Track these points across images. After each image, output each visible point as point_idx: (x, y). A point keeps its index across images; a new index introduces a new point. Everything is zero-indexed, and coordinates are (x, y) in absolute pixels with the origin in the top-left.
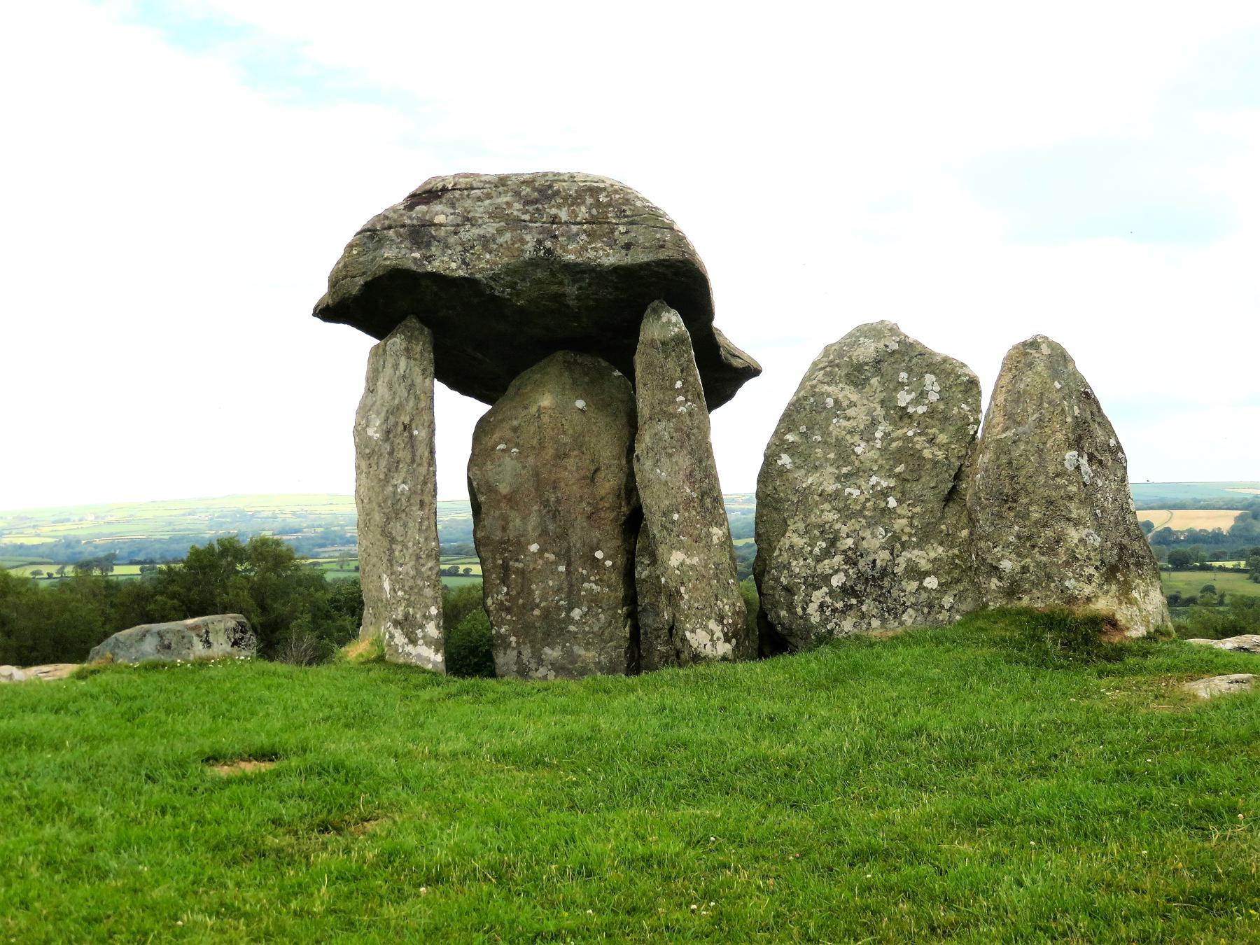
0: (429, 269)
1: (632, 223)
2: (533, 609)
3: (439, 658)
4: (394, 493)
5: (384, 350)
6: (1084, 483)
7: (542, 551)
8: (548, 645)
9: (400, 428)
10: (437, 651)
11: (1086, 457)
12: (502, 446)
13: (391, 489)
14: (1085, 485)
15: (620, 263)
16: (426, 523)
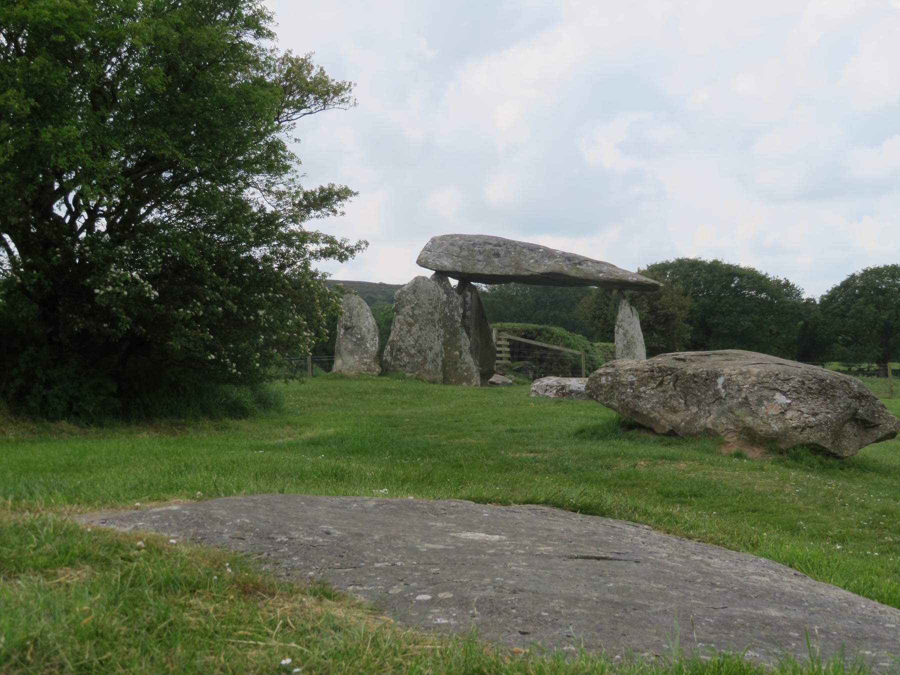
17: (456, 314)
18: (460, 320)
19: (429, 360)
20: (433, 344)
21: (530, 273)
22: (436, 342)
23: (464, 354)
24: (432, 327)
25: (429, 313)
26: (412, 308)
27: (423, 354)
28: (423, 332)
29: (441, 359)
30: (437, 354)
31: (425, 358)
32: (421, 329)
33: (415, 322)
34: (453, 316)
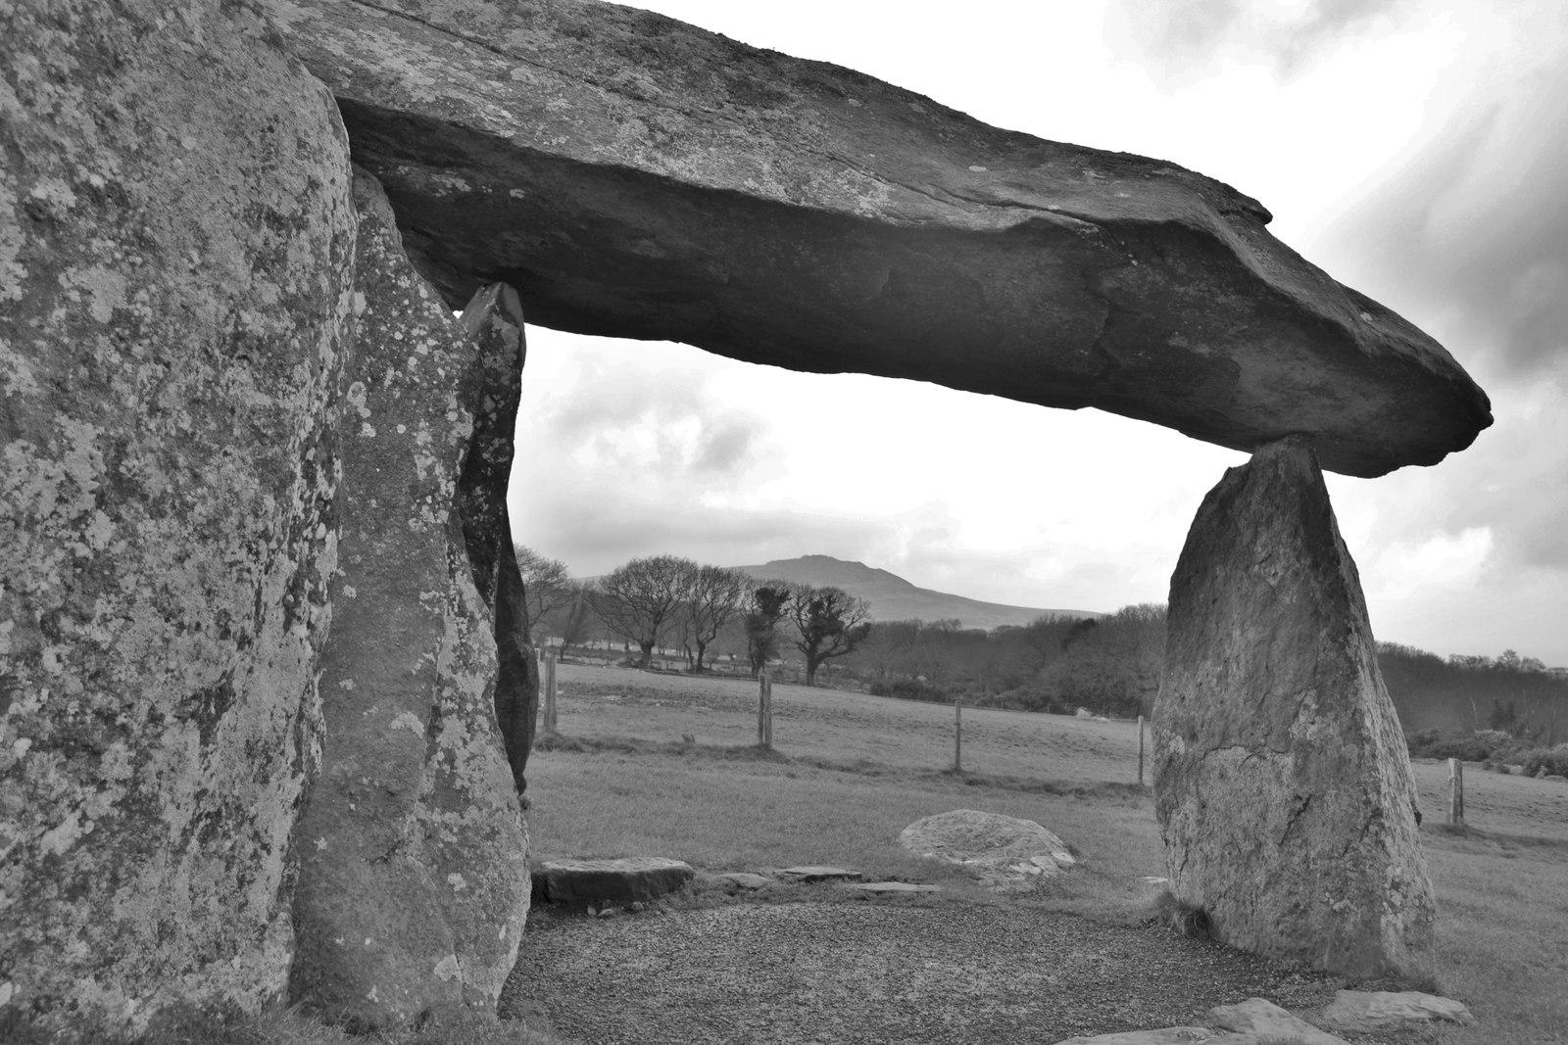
17: (423, 437)
18: (448, 487)
19: (176, 818)
20: (237, 659)
22: (268, 642)
23: (453, 727)
24: (248, 485)
25: (237, 343)
26: (36, 216)
27: (117, 759)
28: (147, 527)
29: (294, 788)
30: (258, 753)
31: (139, 807)
32: (119, 489)
33: (60, 397)
34: (406, 452)
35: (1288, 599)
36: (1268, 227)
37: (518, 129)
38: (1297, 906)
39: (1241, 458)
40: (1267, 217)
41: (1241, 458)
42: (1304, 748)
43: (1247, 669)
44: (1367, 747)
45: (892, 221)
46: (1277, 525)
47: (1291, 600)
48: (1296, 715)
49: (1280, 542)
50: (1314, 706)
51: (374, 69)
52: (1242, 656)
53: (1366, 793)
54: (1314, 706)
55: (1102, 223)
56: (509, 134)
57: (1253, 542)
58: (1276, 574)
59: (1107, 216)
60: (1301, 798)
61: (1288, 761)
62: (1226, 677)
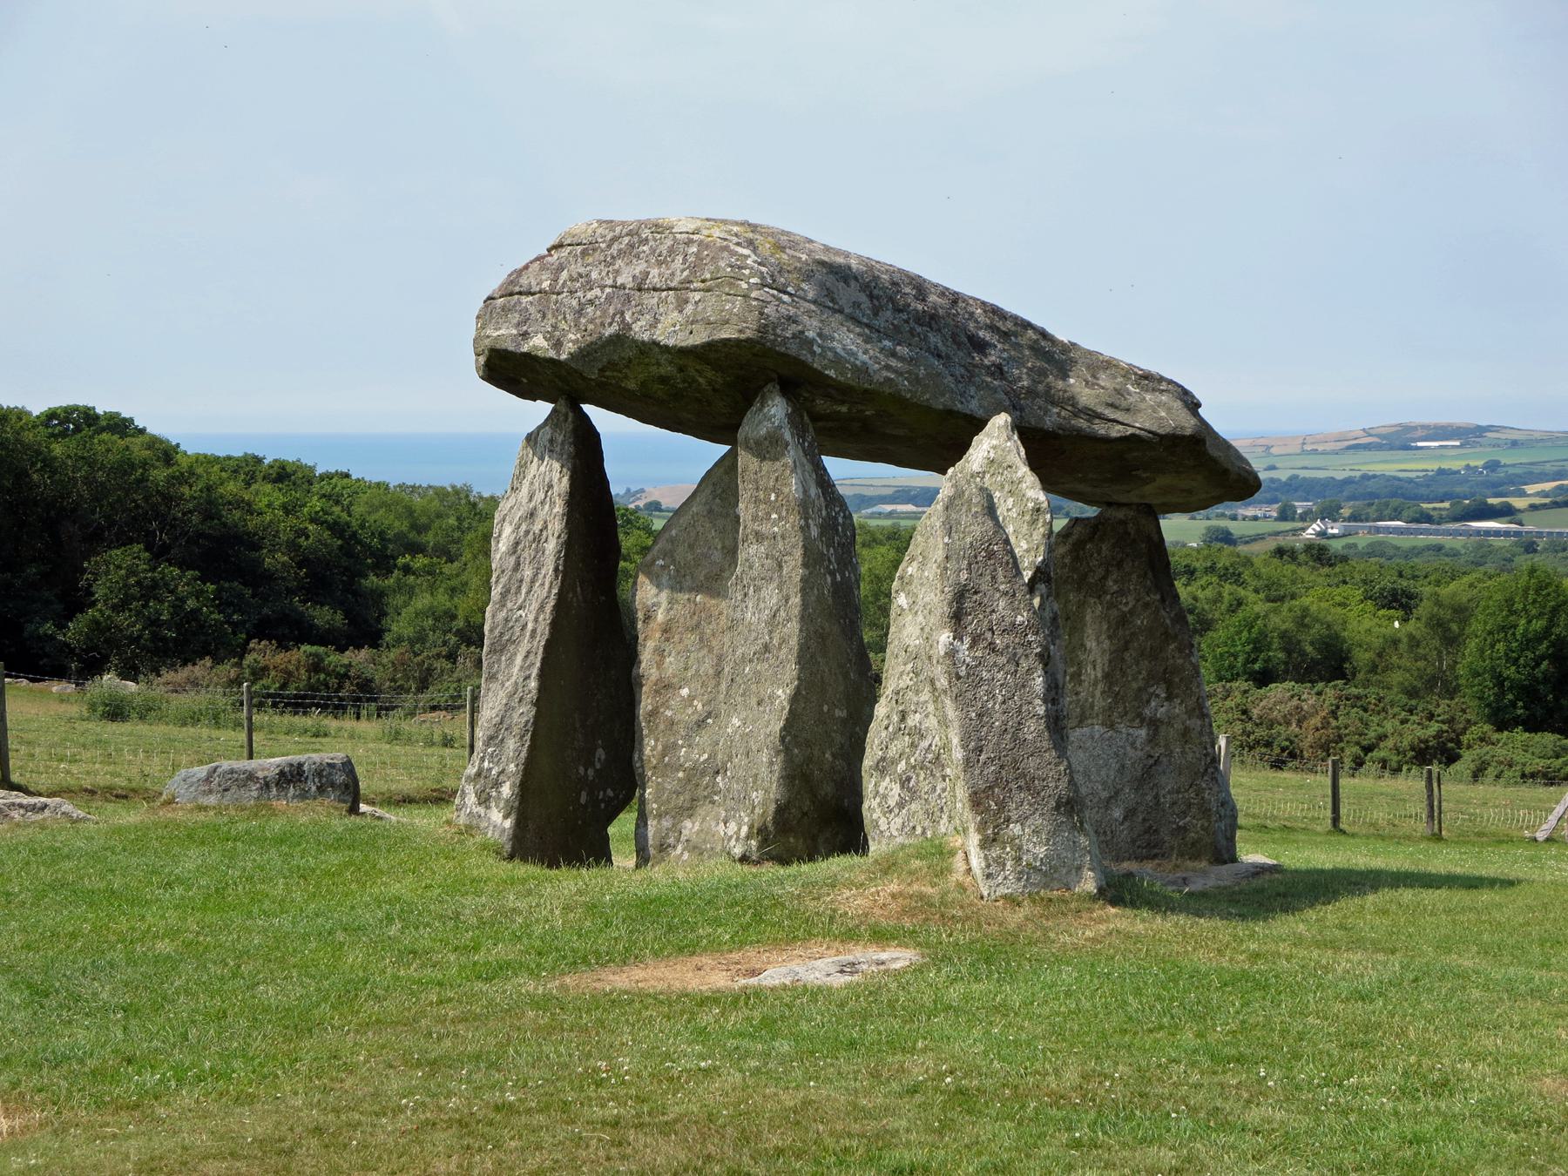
0: (525, 349)
1: (708, 290)
2: (678, 771)
3: (508, 824)
4: (507, 620)
5: (536, 439)
6: (957, 674)
7: (691, 698)
8: (690, 816)
9: (530, 537)
10: (506, 817)
11: (967, 640)
12: (661, 562)
13: (503, 614)
14: (959, 677)
15: (684, 344)
16: (532, 657)
21: (1116, 431)
35: (1139, 622)
36: (1200, 410)
37: (910, 391)
38: (1150, 827)
39: (1091, 512)
40: (1198, 405)
41: (1091, 512)
42: (1154, 724)
43: (1103, 671)
44: (1207, 720)
45: (1061, 432)
46: (1127, 566)
47: (1142, 622)
48: (1148, 702)
49: (1130, 581)
50: (1163, 695)
51: (858, 362)
52: (1099, 661)
53: (1206, 749)
54: (1163, 695)
55: (1162, 437)
56: (909, 396)
57: (1105, 578)
58: (1127, 603)
59: (1161, 431)
60: (1152, 757)
61: (1143, 732)
62: (1080, 675)
